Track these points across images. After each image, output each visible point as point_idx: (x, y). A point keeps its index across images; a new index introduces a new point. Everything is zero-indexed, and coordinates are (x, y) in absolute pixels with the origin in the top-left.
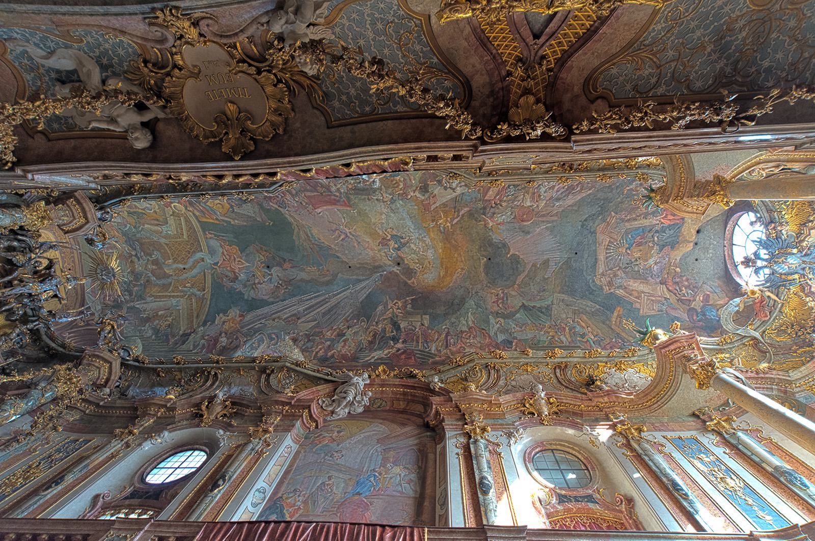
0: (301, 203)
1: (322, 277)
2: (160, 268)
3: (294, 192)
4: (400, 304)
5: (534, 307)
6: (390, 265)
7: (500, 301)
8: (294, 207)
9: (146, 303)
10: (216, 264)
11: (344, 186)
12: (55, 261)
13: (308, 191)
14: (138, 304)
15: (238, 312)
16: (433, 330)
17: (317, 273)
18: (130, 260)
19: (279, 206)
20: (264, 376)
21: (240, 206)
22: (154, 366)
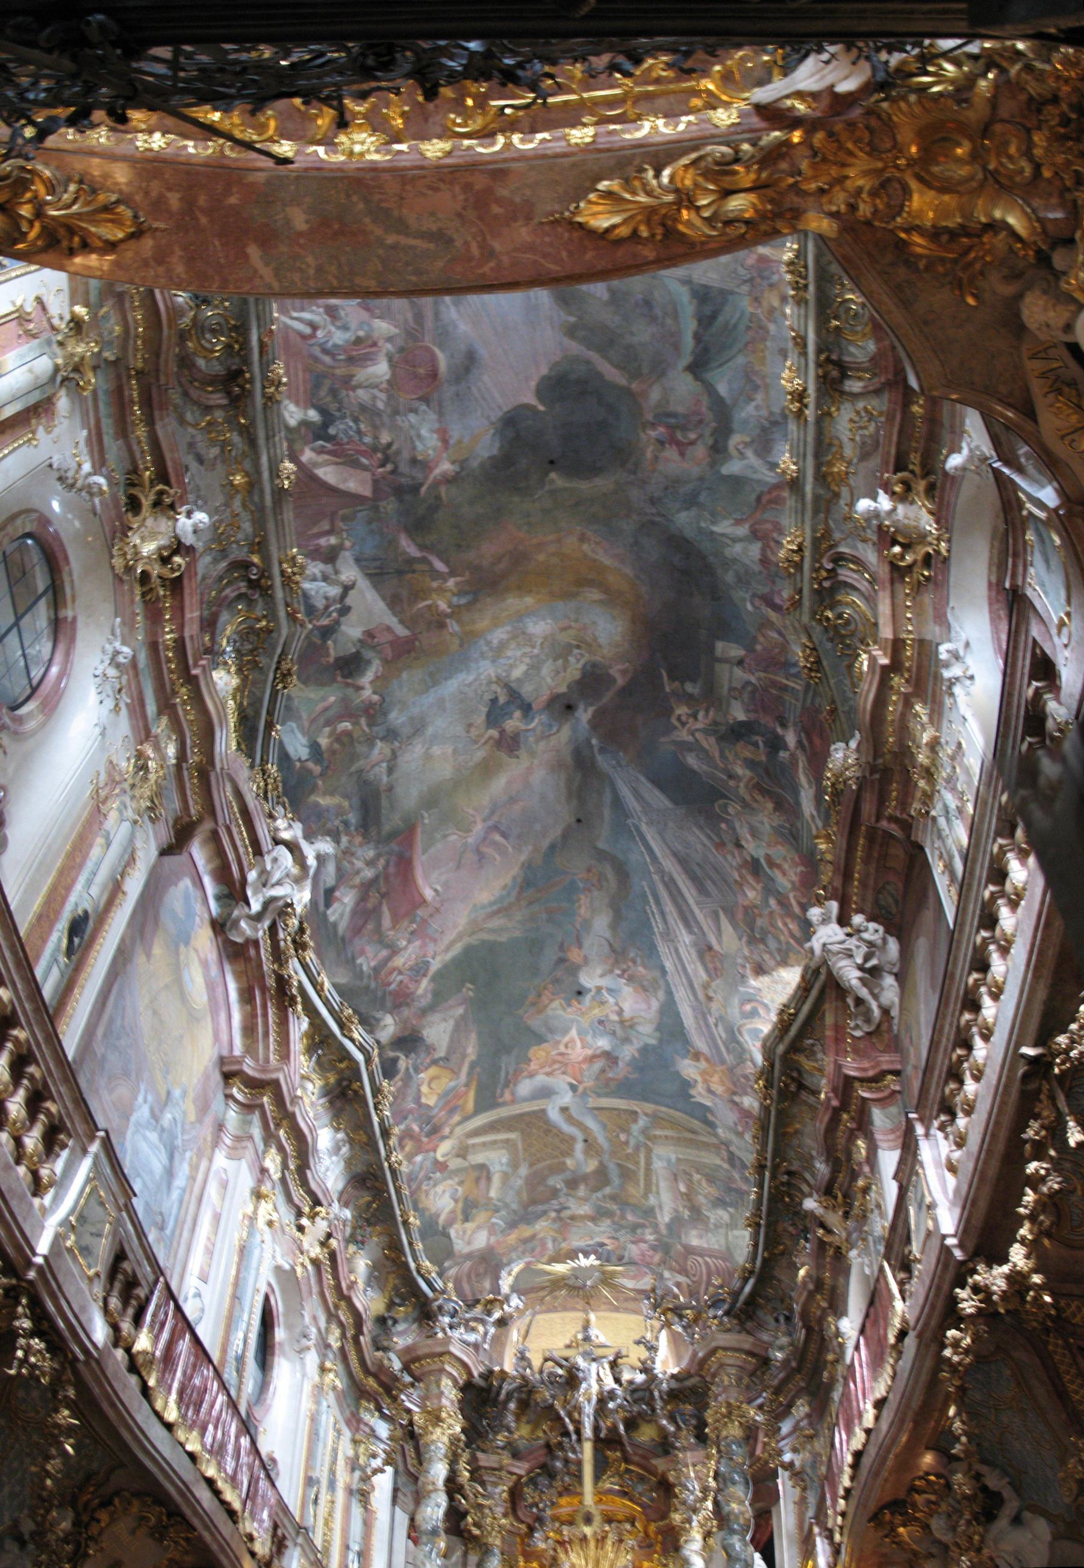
0: (413, 933)
1: (605, 884)
2: (585, 1178)
3: (384, 953)
4: (682, 710)
5: (697, 337)
6: (575, 730)
7: (679, 436)
8: (424, 946)
9: (661, 1207)
10: (573, 1088)
11: (359, 853)
13: (379, 925)
15: (687, 1062)
16: (755, 638)
17: (596, 893)
19: (425, 975)
20: (804, 1095)
21: (430, 1049)
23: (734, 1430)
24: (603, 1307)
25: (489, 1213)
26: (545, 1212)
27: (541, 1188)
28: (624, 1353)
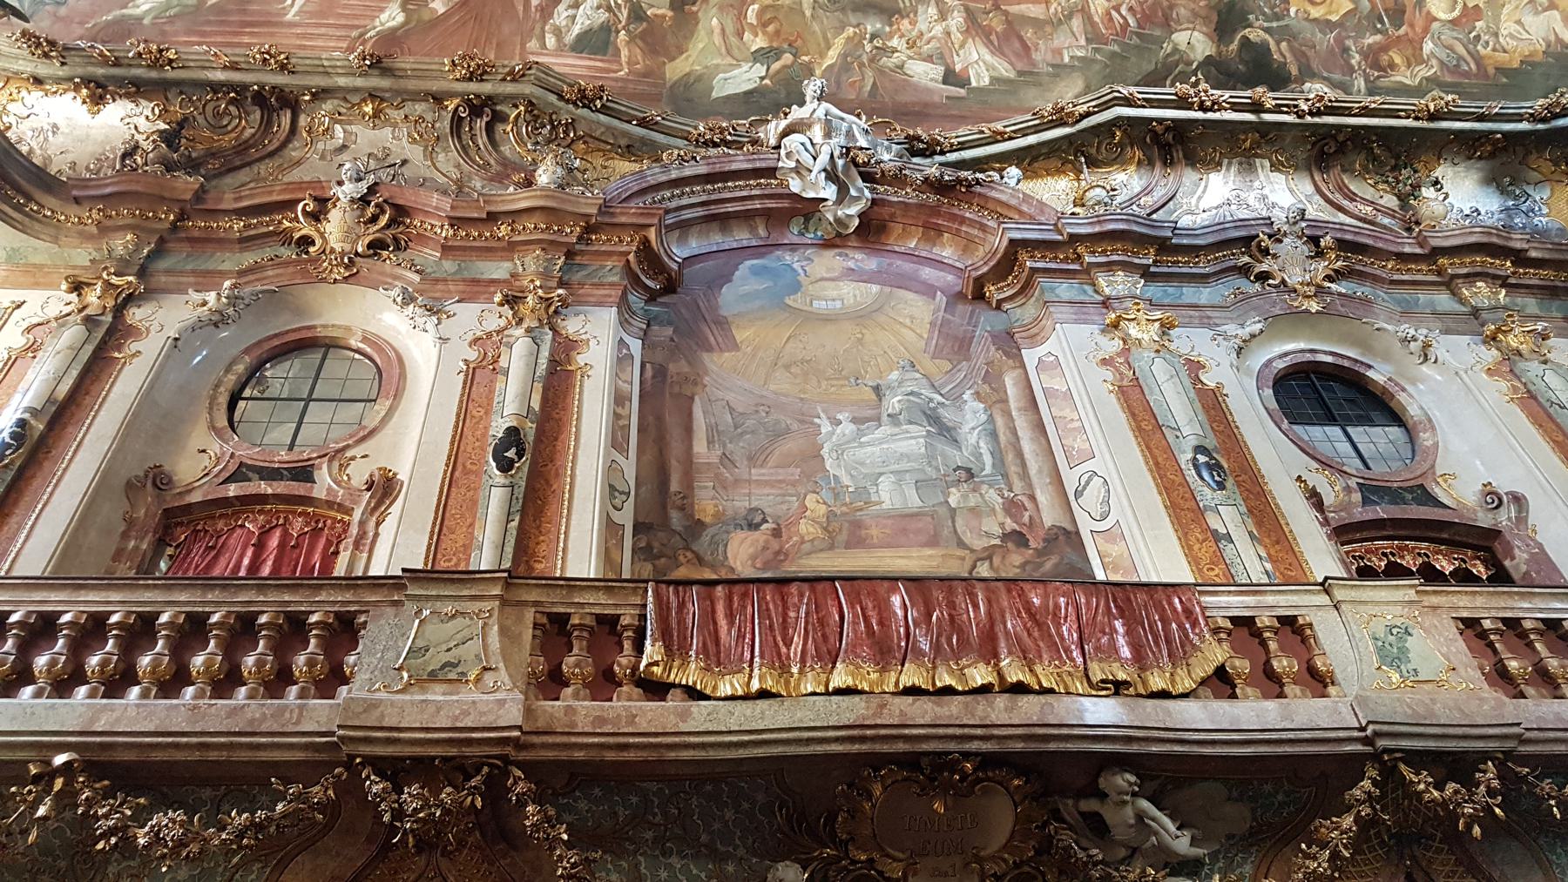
3: (1076, 23)
13: (1037, 23)
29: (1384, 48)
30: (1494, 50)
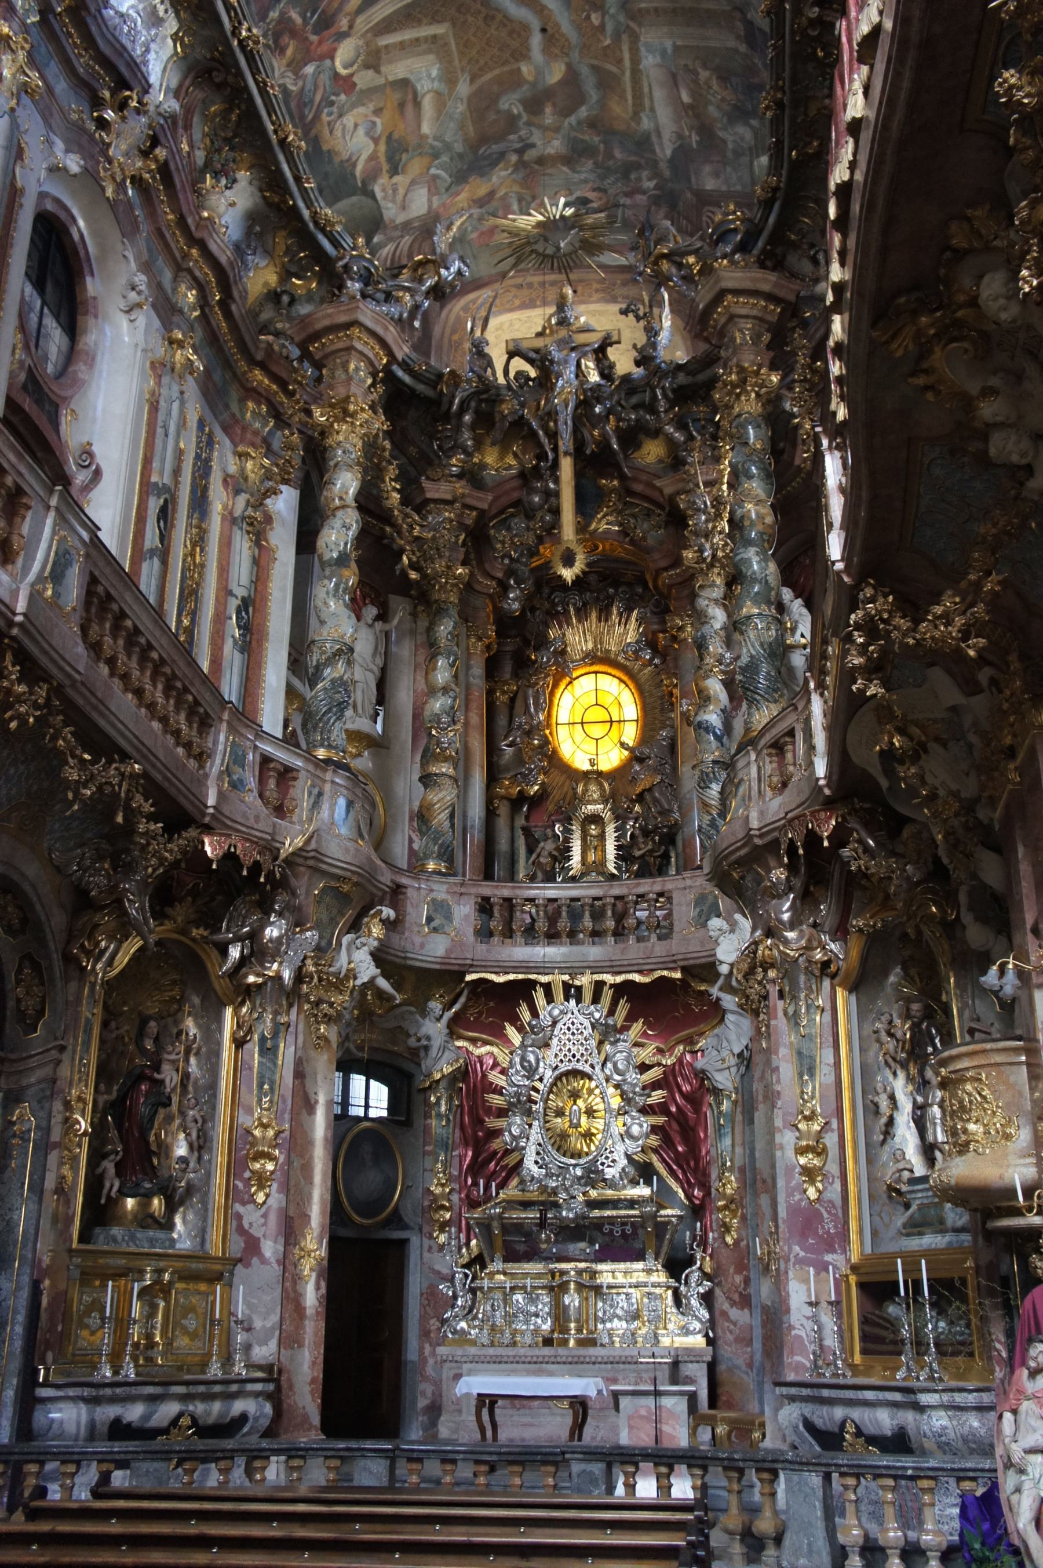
12: (511, 347)
14: (663, 149)
18: (536, 167)
22: (785, 165)
23: (749, 405)
24: (596, 297)
25: (426, 160)
26: (502, 155)
27: (492, 116)
28: (615, 338)
29: (293, 33)
30: (329, 123)
